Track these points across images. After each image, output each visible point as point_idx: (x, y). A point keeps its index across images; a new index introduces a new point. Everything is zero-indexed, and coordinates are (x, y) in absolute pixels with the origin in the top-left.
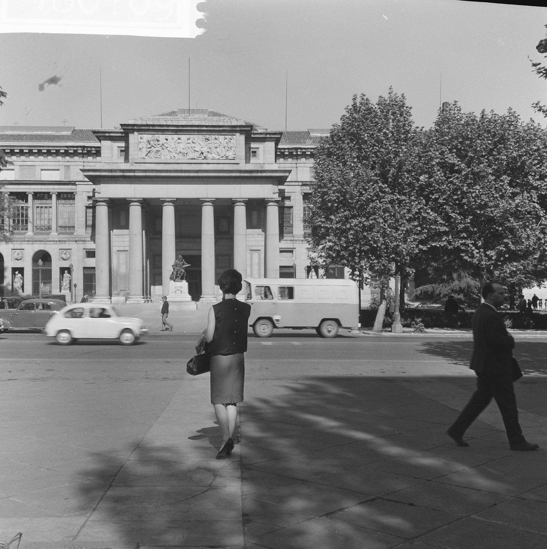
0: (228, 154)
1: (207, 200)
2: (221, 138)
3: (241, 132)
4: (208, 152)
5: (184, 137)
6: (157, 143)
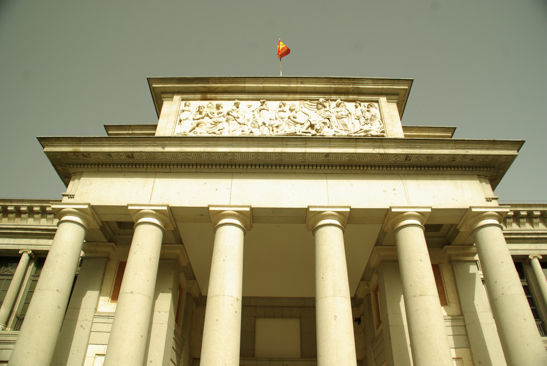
0: (366, 128)
1: (329, 211)
2: (350, 106)
3: (389, 94)
4: (325, 123)
5: (273, 105)
6: (216, 111)
